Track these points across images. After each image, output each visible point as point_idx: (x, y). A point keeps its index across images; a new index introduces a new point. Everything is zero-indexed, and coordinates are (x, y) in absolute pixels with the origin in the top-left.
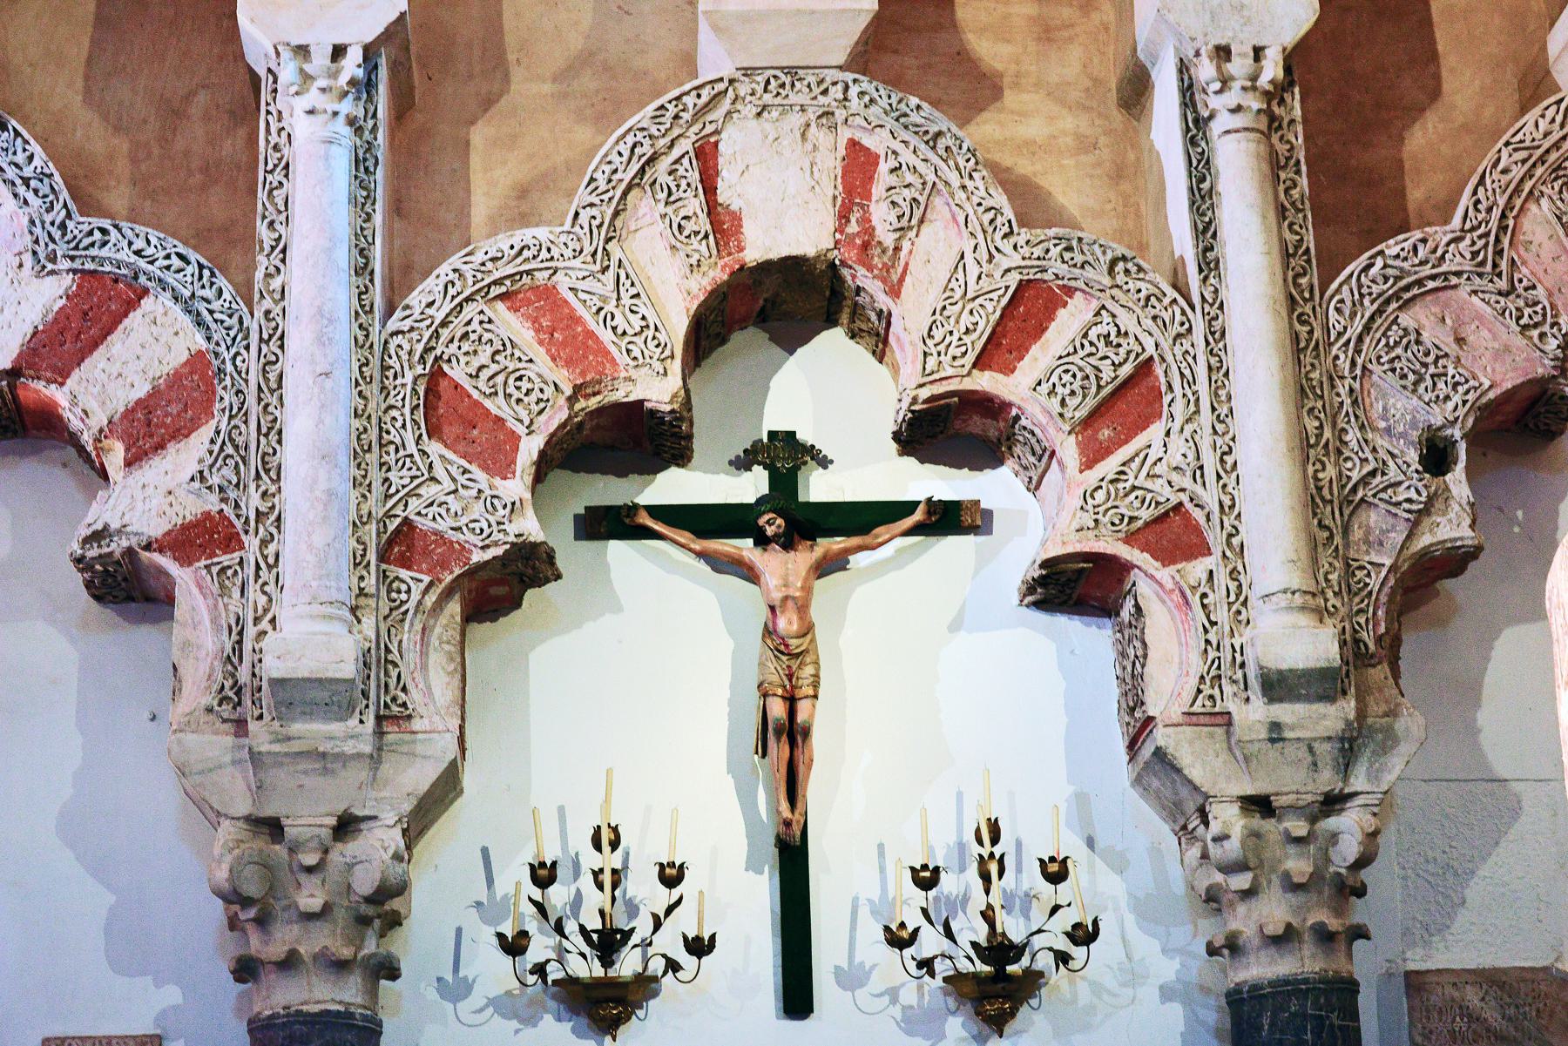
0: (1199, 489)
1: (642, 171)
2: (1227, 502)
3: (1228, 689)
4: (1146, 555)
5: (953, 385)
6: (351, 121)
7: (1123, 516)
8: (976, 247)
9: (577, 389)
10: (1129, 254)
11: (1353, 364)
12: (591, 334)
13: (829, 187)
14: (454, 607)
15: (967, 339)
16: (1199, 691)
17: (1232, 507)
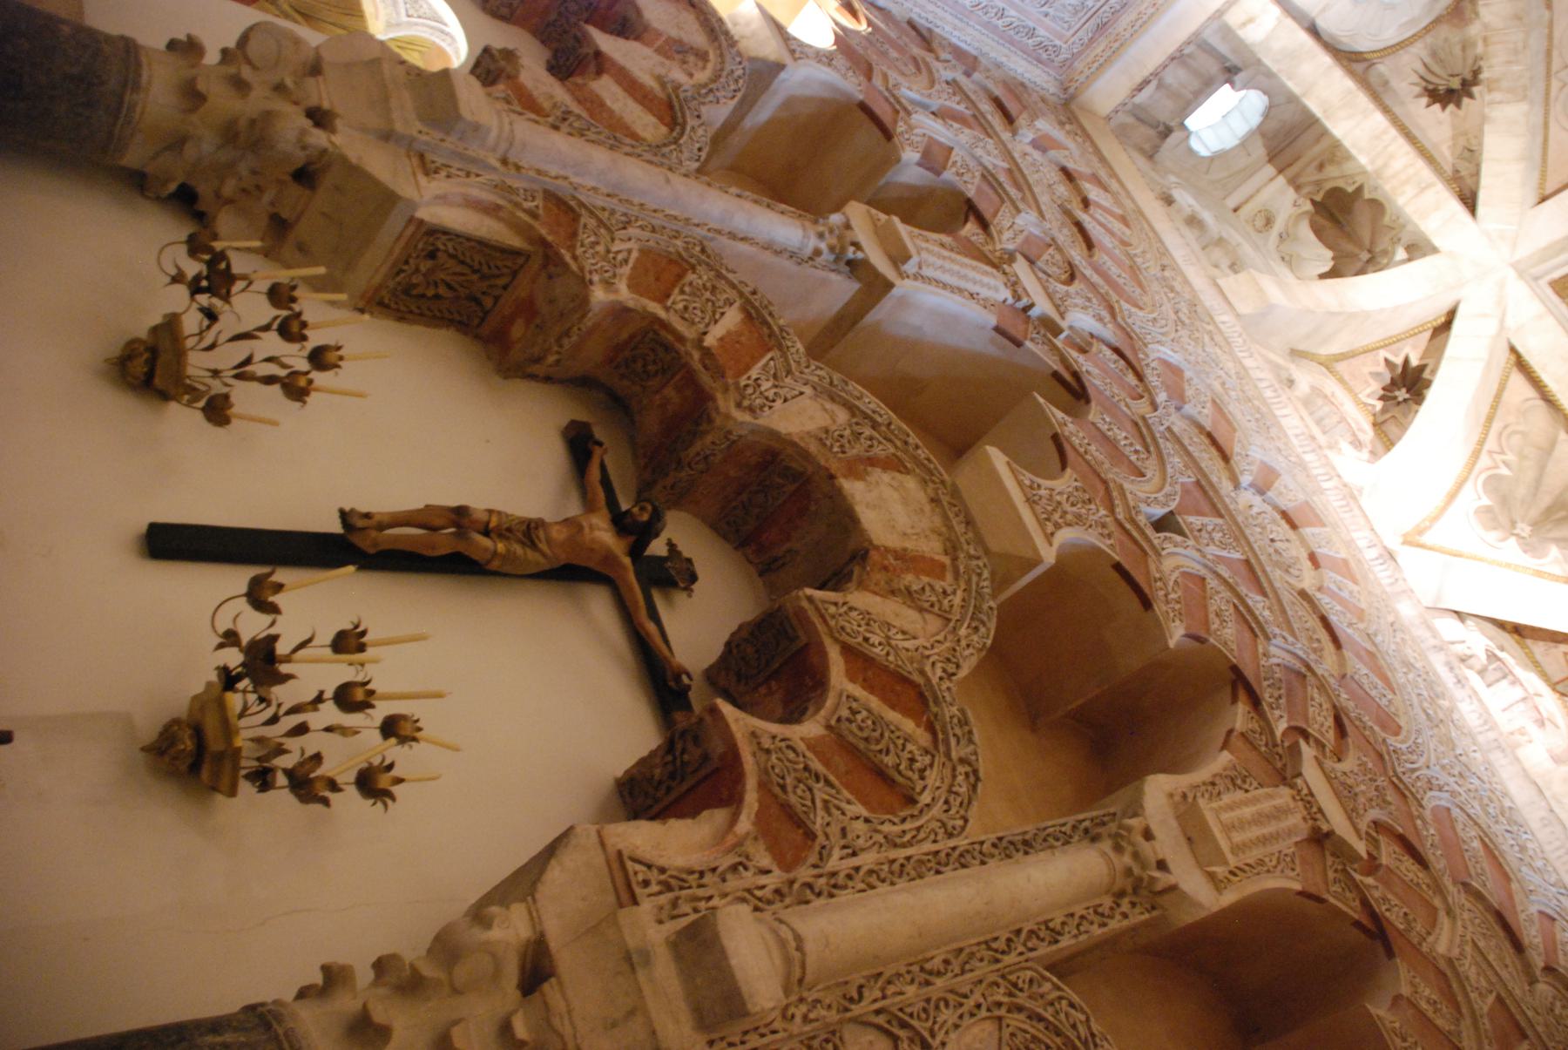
0: (837, 853)
1: (866, 416)
2: (841, 879)
3: (664, 899)
4: (756, 806)
5: (820, 627)
6: (817, 252)
7: (783, 778)
8: (925, 648)
9: (707, 353)
10: (981, 775)
11: (999, 1004)
12: (748, 368)
13: (909, 545)
14: (516, 242)
15: (860, 639)
16: (649, 867)
17: (835, 886)
